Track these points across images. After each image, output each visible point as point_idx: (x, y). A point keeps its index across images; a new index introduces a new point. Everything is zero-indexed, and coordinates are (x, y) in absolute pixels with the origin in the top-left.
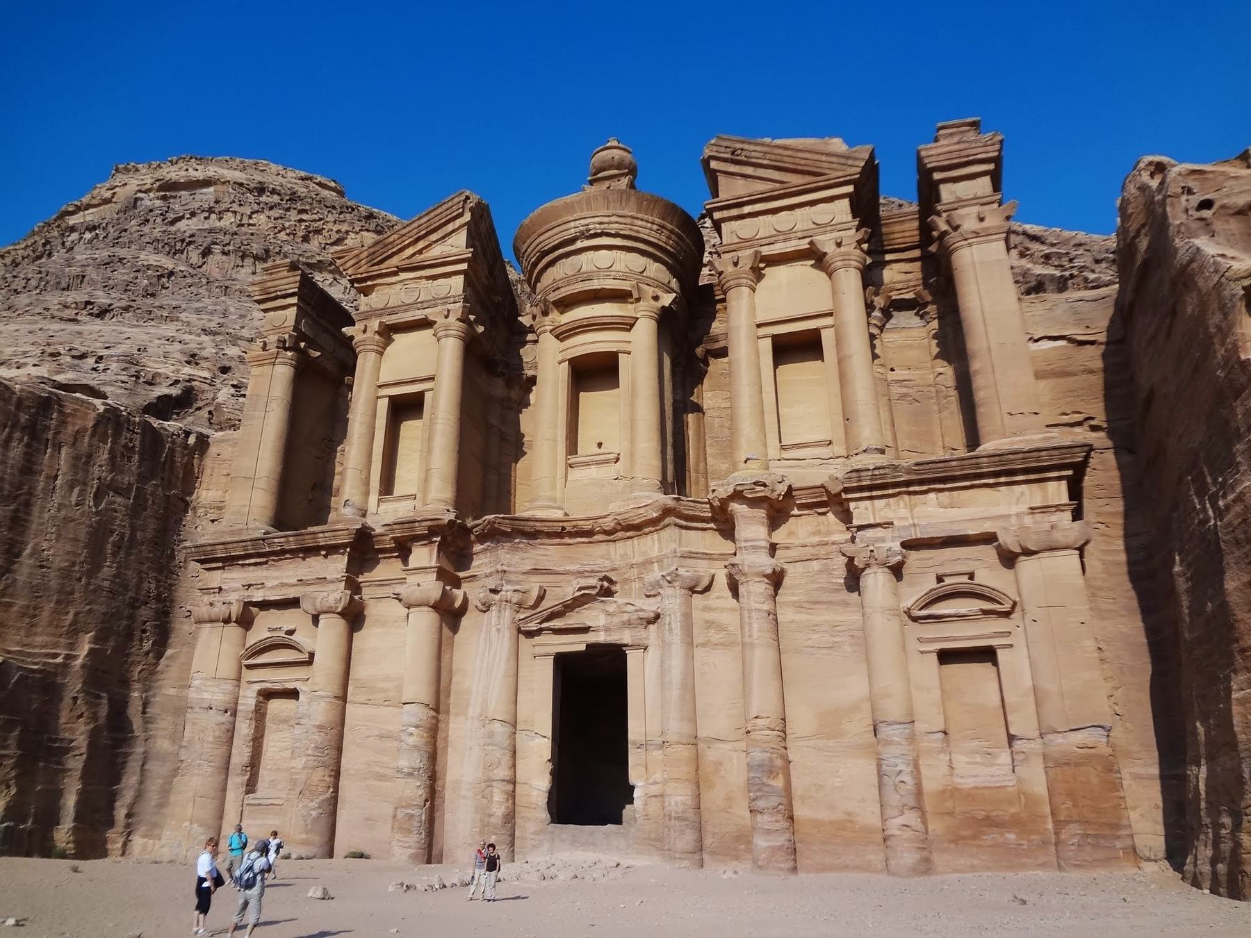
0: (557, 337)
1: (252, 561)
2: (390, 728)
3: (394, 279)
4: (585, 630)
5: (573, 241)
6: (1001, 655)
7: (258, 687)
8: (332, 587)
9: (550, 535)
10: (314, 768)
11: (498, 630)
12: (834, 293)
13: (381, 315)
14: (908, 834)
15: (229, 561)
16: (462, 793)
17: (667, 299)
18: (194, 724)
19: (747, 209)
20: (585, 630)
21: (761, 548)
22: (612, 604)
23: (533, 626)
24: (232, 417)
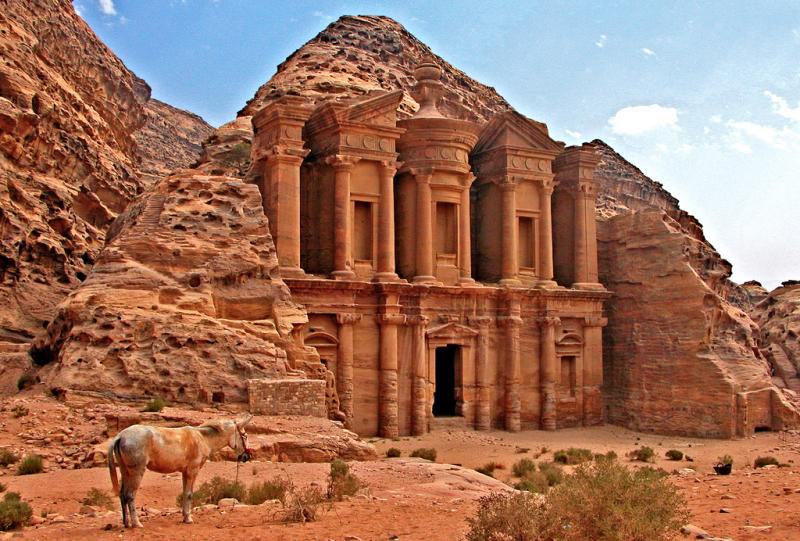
2: (370, 378)
3: (361, 131)
5: (449, 141)
12: (541, 205)
19: (519, 153)
20: (449, 338)
23: (433, 336)
24: (14, 88)
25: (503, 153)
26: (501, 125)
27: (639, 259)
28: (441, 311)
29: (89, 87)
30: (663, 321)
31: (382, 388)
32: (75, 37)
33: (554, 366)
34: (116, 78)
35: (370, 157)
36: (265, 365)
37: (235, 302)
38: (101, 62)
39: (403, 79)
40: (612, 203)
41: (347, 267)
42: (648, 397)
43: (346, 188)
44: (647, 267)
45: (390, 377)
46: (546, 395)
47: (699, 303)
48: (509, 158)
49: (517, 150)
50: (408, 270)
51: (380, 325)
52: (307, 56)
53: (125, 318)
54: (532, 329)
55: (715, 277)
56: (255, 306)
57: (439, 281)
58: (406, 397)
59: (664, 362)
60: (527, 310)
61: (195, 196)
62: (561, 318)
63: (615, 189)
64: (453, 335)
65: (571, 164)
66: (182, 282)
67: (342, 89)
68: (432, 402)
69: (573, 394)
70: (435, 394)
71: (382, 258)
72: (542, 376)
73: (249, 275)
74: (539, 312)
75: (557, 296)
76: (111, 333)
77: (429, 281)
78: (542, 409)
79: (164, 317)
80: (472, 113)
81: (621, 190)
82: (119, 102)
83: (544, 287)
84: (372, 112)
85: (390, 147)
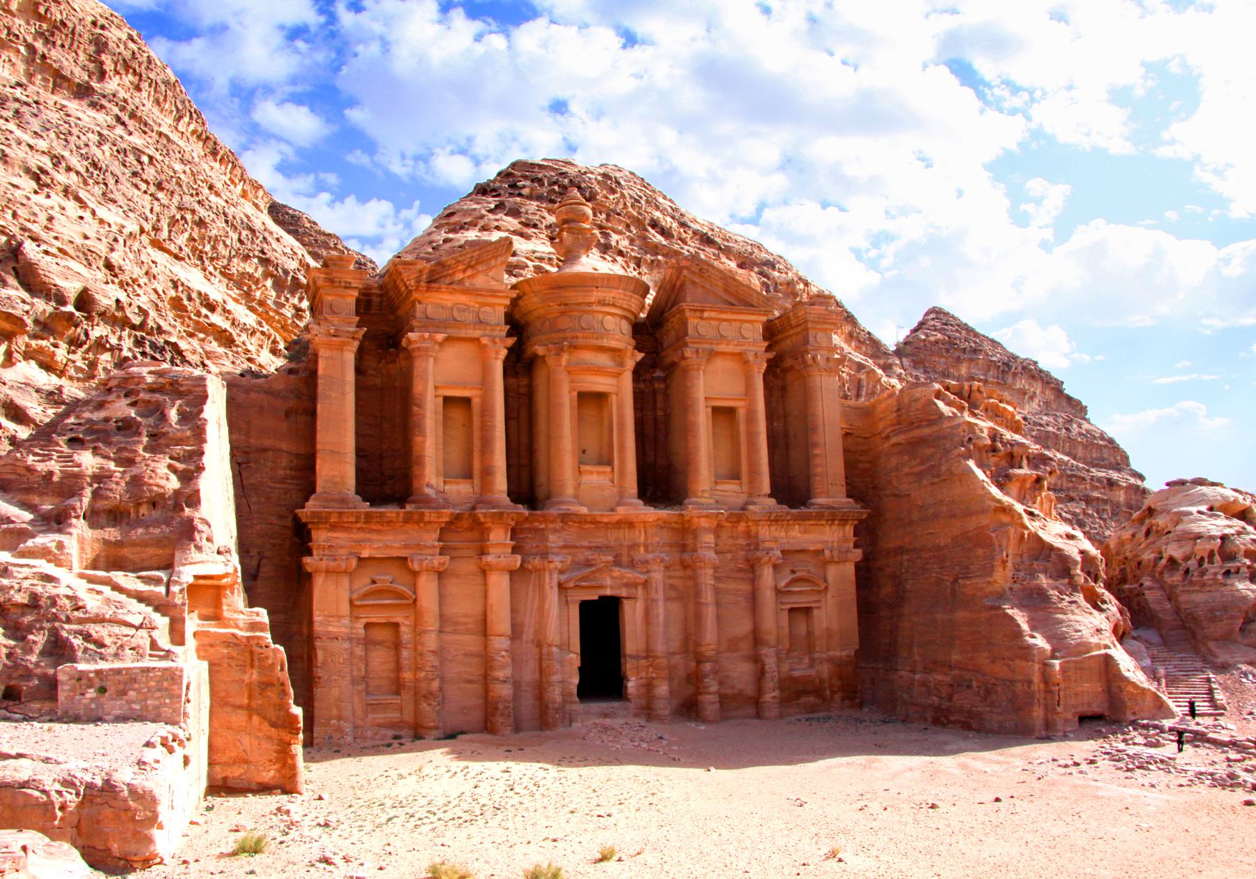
0: (569, 372)
1: (358, 525)
2: (472, 649)
4: (601, 587)
5: (590, 304)
6: (816, 612)
7: (364, 621)
8: (430, 551)
9: (575, 522)
10: (433, 679)
11: (552, 587)
13: (438, 327)
14: (775, 700)
15: (334, 527)
16: (523, 688)
17: (640, 356)
18: (325, 650)
19: (706, 314)
20: (601, 587)
21: (710, 547)
22: (617, 572)
23: (571, 584)
24: (47, 280)
26: (678, 277)
27: (906, 458)
28: (590, 548)
29: (246, 284)
30: (938, 548)
31: (487, 661)
32: (224, 225)
33: (773, 619)
34: (286, 272)
35: (462, 334)
36: (108, 641)
38: (262, 252)
41: (427, 490)
42: (919, 667)
43: (427, 381)
44: (916, 470)
45: (497, 646)
46: (763, 665)
48: (693, 322)
49: (703, 311)
50: (541, 493)
52: (452, 214)
54: (740, 570)
55: (1023, 479)
56: (151, 551)
57: (582, 504)
58: (529, 674)
60: (730, 542)
61: (118, 397)
62: (782, 552)
63: (958, 370)
64: (609, 582)
65: (797, 326)
68: (576, 680)
69: (813, 662)
70: (580, 669)
71: (487, 472)
72: (757, 638)
74: (749, 545)
78: (760, 690)
81: (969, 372)
82: (296, 301)
83: (751, 507)
84: (464, 271)
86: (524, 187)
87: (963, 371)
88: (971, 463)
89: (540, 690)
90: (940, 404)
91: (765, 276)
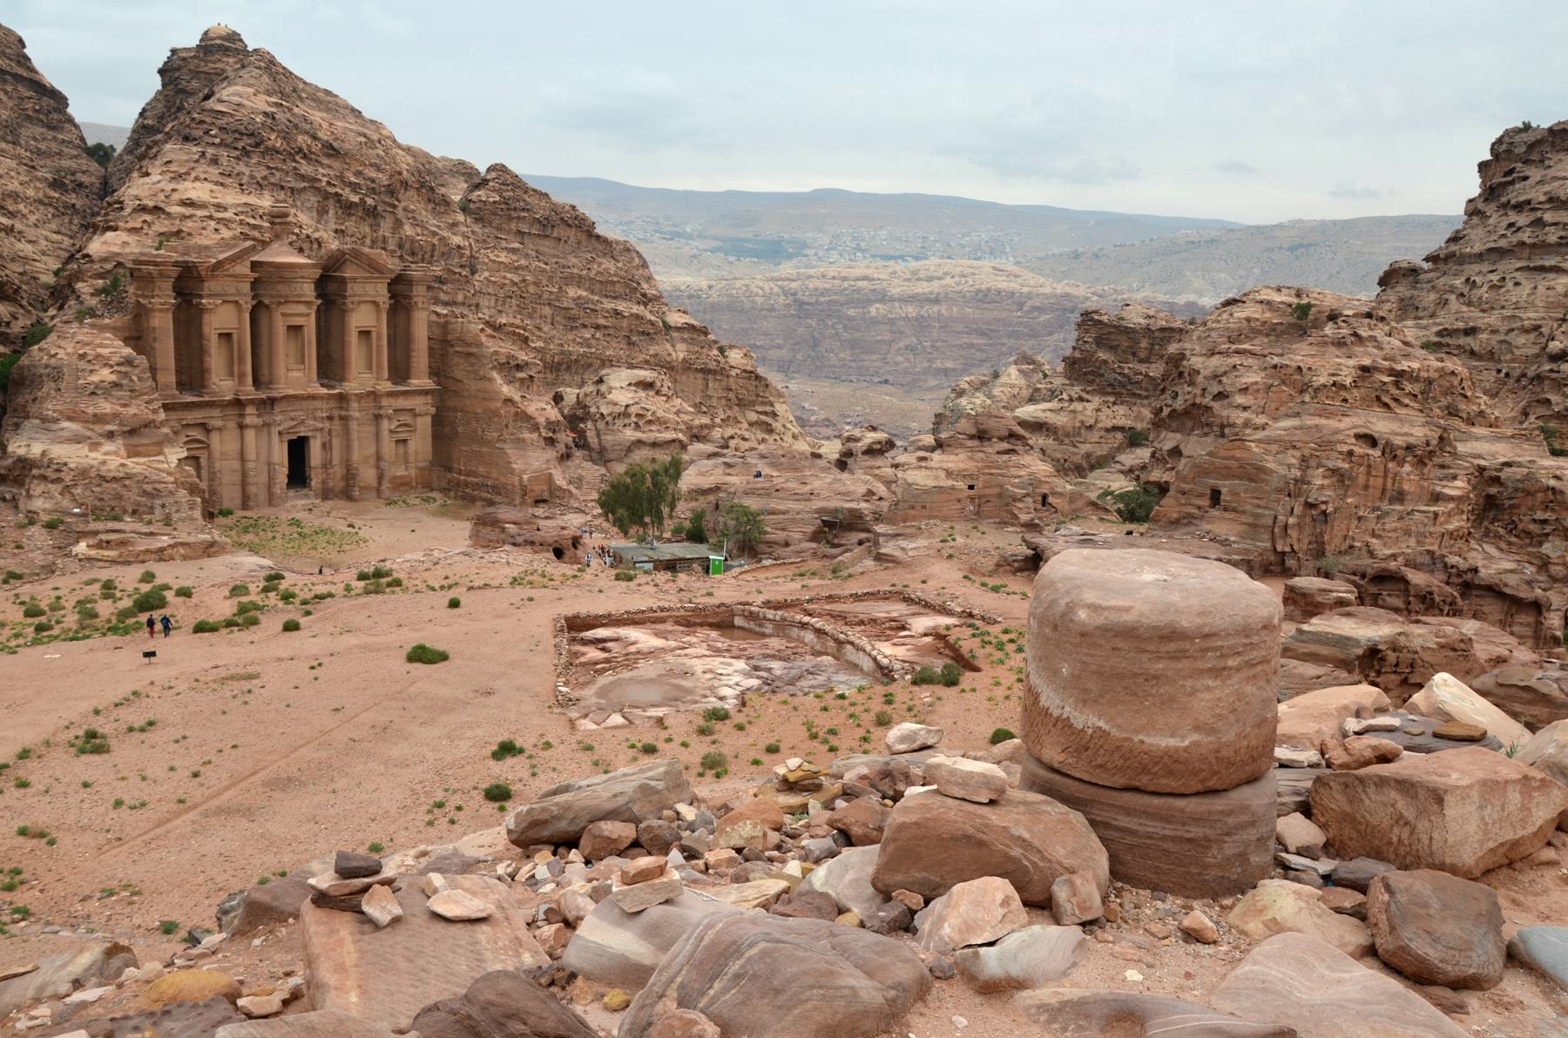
12: (378, 320)
25: (343, 281)
30: (476, 414)
31: (244, 474)
35: (229, 299)
37: (137, 446)
39: (264, 178)
40: (504, 244)
47: (499, 405)
48: (349, 286)
50: (265, 379)
51: (242, 427)
52: (170, 162)
53: (72, 466)
55: (522, 380)
58: (263, 479)
59: (476, 447)
66: (101, 435)
67: (203, 206)
69: (407, 469)
71: (242, 375)
72: (379, 458)
73: (146, 426)
75: (391, 394)
76: (62, 475)
77: (283, 389)
79: (95, 463)
80: (337, 194)
85: (246, 288)
86: (215, 137)
87: (513, 226)
88: (495, 374)
89: (270, 488)
90: (483, 338)
91: (373, 181)
